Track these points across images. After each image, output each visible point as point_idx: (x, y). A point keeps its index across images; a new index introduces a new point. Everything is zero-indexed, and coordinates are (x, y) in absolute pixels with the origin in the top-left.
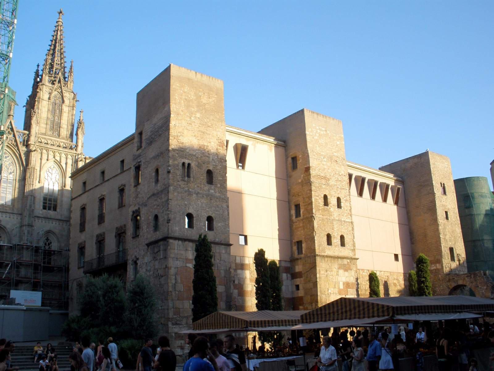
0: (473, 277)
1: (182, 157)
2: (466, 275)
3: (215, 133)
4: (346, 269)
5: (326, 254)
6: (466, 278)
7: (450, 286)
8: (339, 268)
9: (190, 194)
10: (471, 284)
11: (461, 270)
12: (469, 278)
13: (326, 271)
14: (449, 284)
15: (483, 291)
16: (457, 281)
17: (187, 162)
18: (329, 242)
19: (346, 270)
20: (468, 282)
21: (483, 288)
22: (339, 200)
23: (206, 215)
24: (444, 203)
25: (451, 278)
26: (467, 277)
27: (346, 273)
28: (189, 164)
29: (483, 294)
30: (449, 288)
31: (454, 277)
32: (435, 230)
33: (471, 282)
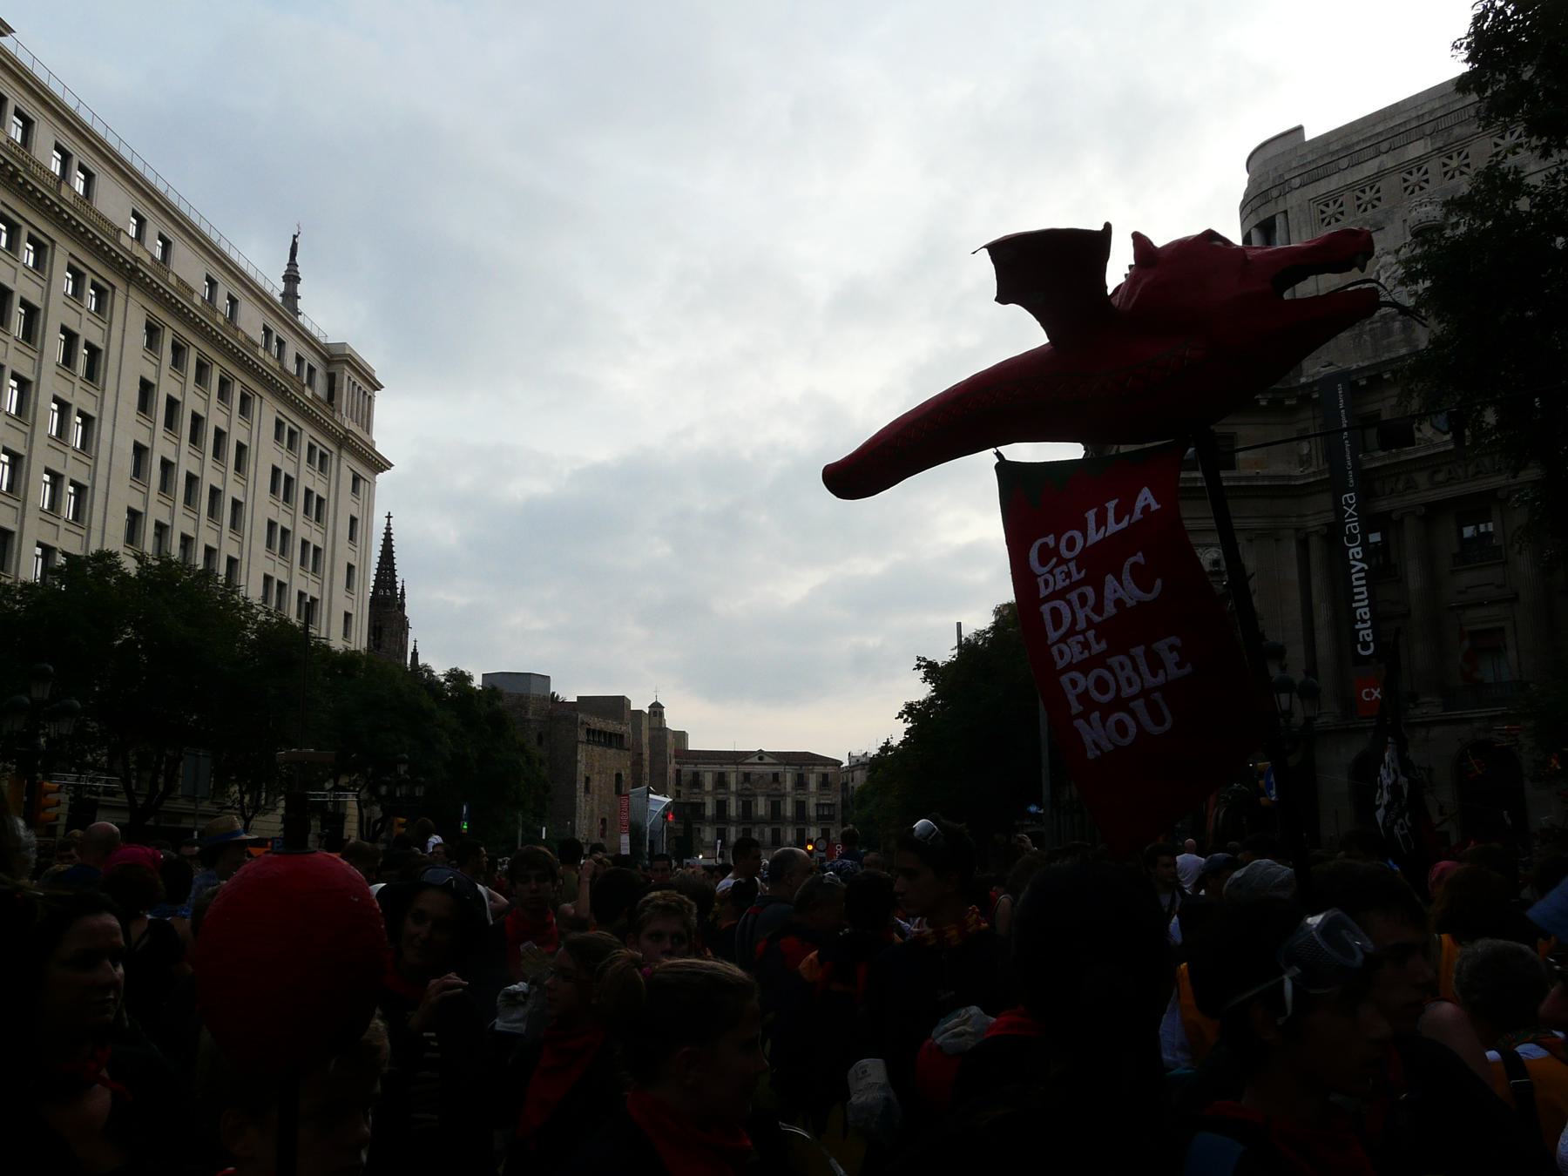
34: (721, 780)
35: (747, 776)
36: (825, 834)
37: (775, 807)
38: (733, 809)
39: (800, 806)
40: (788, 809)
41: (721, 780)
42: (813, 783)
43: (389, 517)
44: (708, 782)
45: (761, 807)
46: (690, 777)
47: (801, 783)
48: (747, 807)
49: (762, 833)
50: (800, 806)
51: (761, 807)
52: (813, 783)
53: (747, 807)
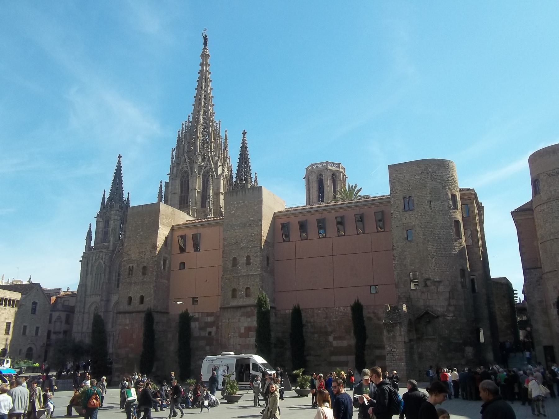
1: (128, 264)
3: (150, 241)
4: (248, 315)
5: (229, 306)
8: (242, 316)
9: (131, 284)
11: (430, 298)
13: (229, 319)
17: (131, 265)
18: (234, 296)
19: (249, 317)
22: (248, 258)
23: (140, 295)
24: (405, 221)
27: (249, 320)
28: (133, 266)
43: (244, 133)
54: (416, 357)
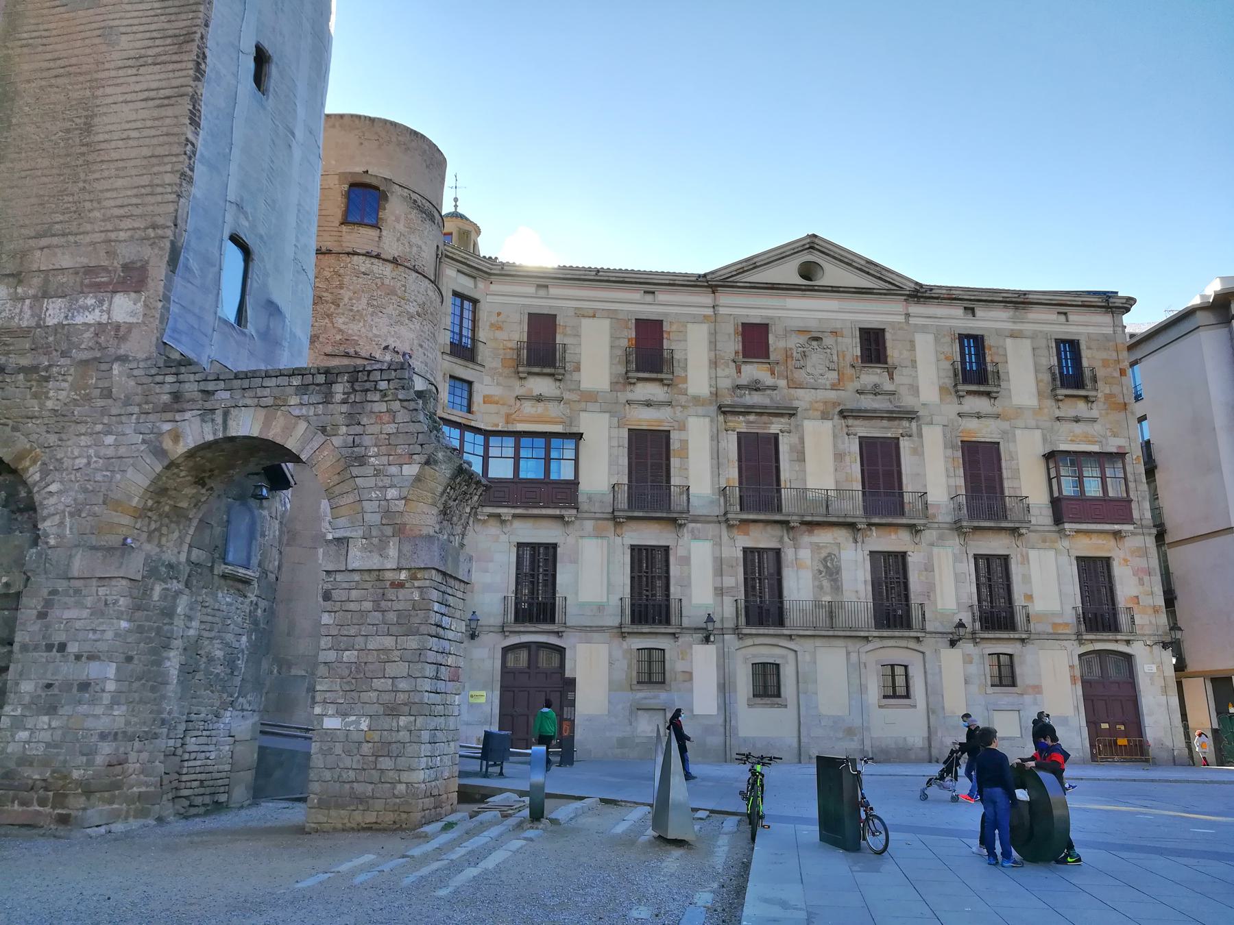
0: (339, 397)
2: (296, 381)
6: (294, 400)
7: (167, 444)
10: (320, 438)
12: (314, 399)
14: (167, 427)
15: (392, 493)
16: (226, 414)
20: (303, 425)
21: (393, 470)
25: (191, 388)
26: (303, 389)
29: (387, 513)
30: (159, 452)
31: (211, 386)
32: (162, 93)
33: (323, 430)
34: (648, 352)
35: (755, 339)
36: (1095, 575)
37: (881, 467)
38: (703, 467)
39: (981, 464)
40: (933, 475)
41: (648, 352)
42: (1023, 373)
44: (595, 353)
45: (820, 463)
46: (518, 333)
47: (975, 369)
48: (759, 463)
49: (830, 570)
50: (981, 464)
51: (820, 463)
52: (1023, 373)
53: (759, 463)
54: (173, 662)
